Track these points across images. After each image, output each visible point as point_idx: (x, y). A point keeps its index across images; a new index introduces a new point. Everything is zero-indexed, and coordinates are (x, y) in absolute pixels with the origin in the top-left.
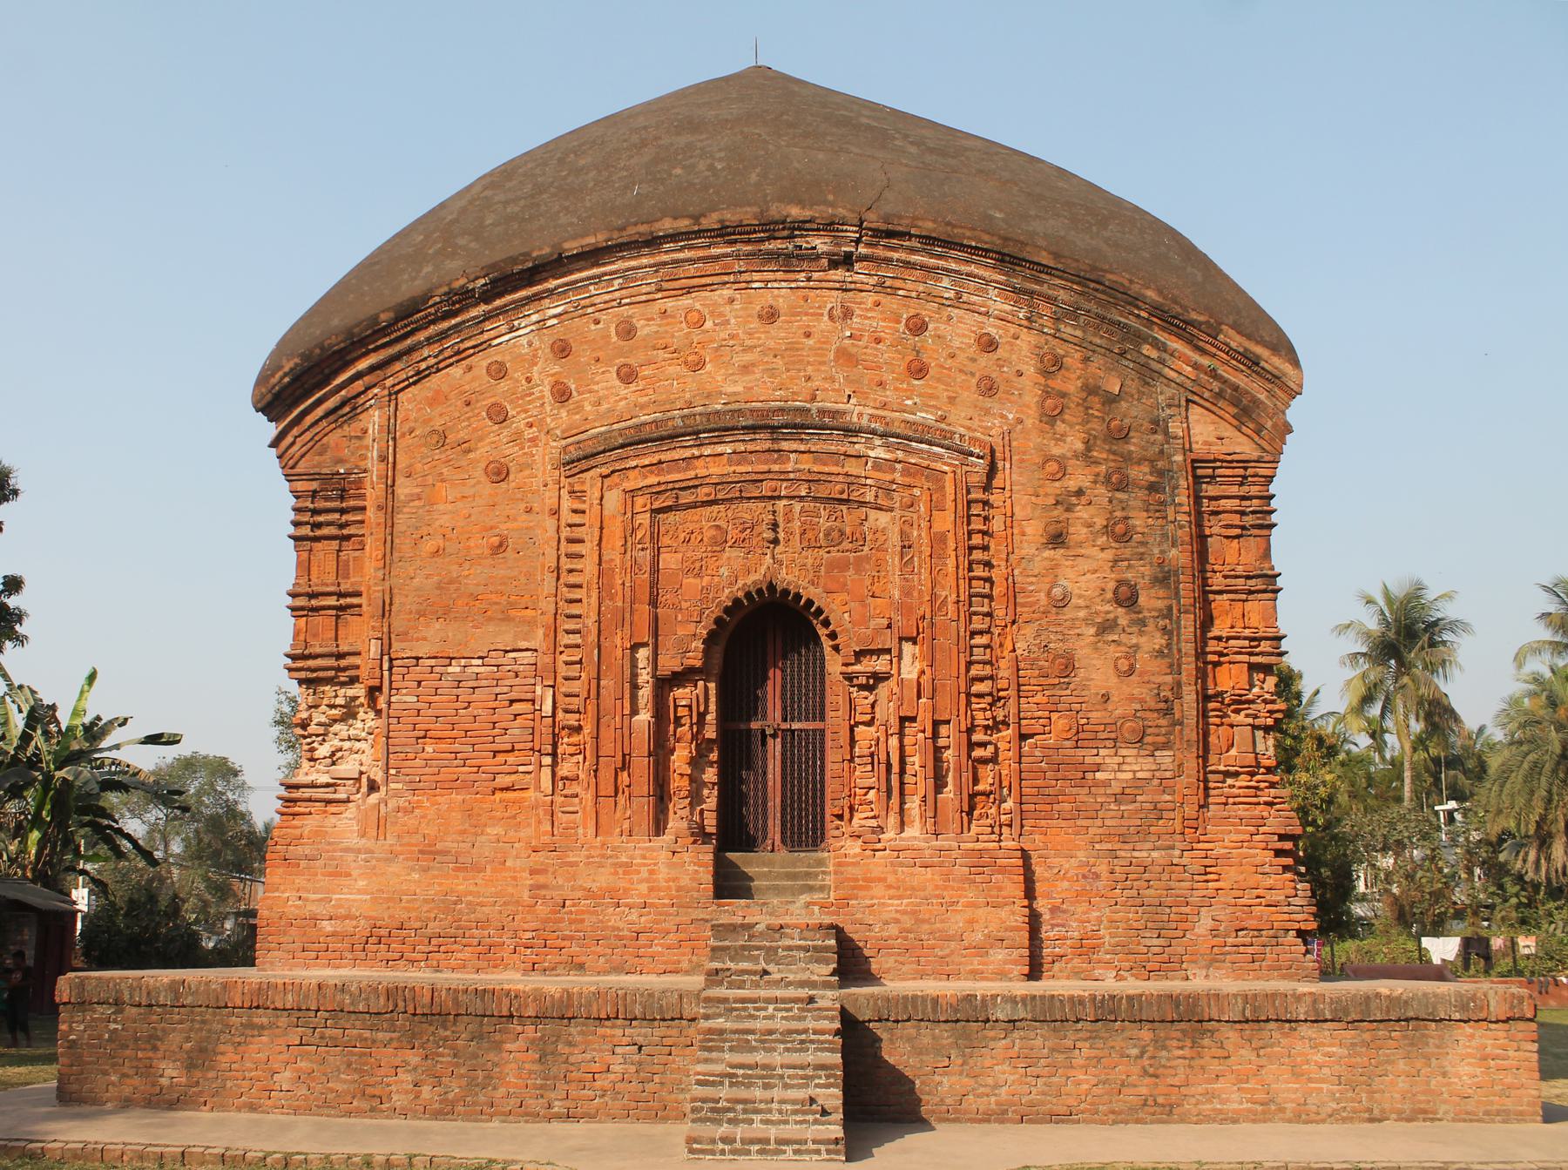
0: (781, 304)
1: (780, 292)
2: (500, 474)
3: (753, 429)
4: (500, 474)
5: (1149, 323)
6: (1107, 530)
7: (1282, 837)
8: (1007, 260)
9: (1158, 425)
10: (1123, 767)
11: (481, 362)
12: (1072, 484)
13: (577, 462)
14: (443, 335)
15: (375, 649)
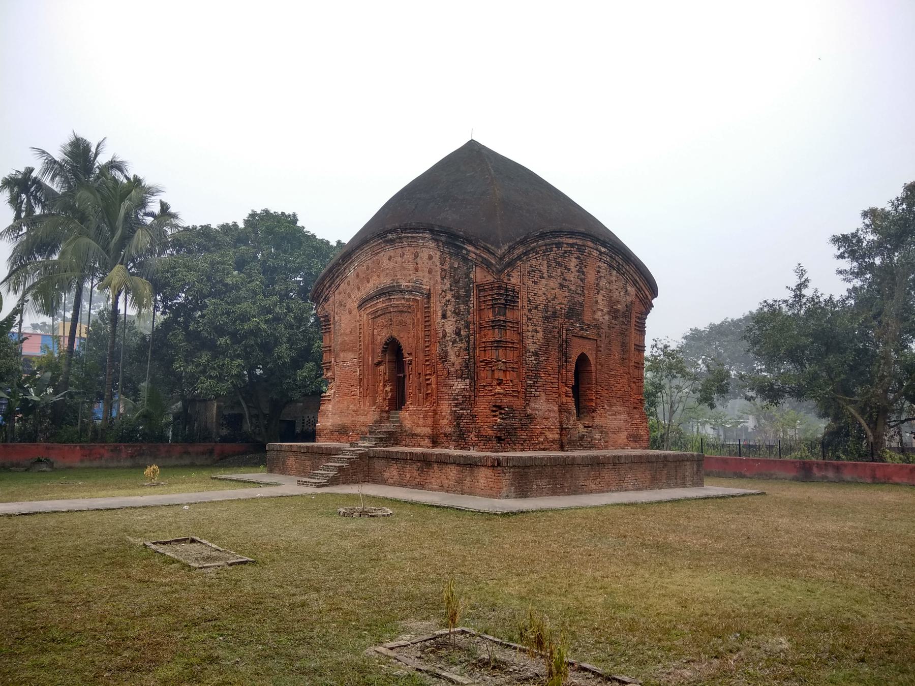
0: (392, 254)
1: (390, 251)
2: (350, 313)
3: (385, 293)
4: (350, 313)
5: (464, 243)
6: (454, 312)
7: (494, 406)
8: (431, 231)
9: (467, 275)
10: (459, 385)
11: (346, 281)
12: (447, 298)
13: (360, 307)
14: (338, 276)
15: (333, 360)
